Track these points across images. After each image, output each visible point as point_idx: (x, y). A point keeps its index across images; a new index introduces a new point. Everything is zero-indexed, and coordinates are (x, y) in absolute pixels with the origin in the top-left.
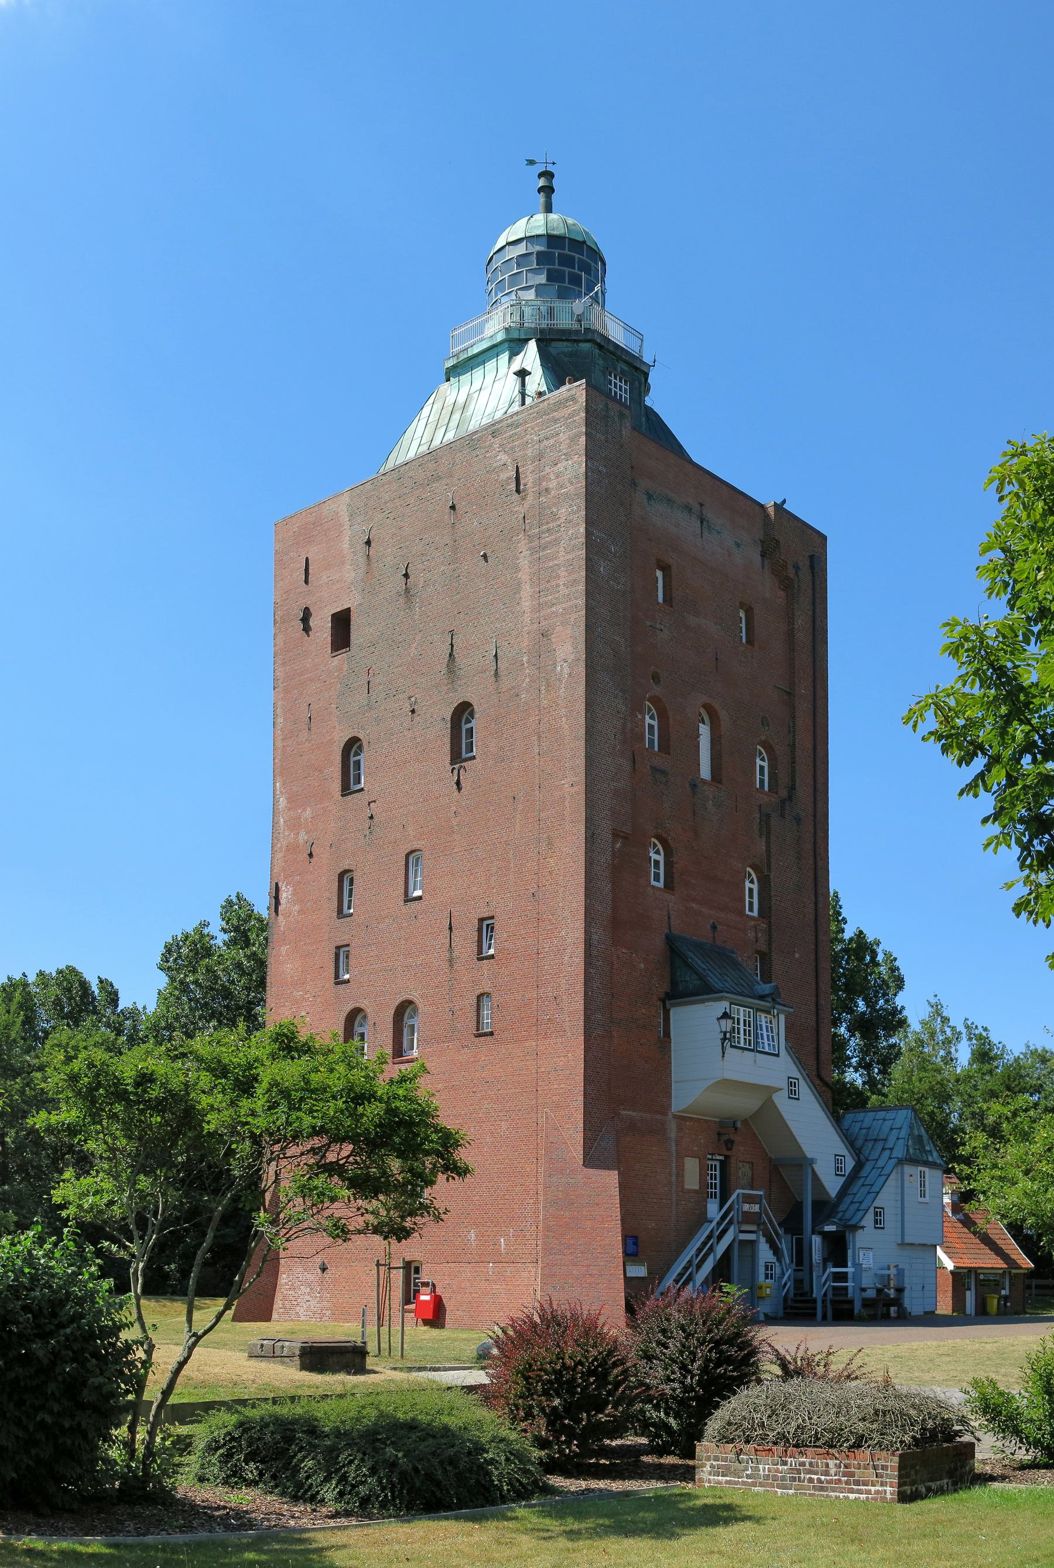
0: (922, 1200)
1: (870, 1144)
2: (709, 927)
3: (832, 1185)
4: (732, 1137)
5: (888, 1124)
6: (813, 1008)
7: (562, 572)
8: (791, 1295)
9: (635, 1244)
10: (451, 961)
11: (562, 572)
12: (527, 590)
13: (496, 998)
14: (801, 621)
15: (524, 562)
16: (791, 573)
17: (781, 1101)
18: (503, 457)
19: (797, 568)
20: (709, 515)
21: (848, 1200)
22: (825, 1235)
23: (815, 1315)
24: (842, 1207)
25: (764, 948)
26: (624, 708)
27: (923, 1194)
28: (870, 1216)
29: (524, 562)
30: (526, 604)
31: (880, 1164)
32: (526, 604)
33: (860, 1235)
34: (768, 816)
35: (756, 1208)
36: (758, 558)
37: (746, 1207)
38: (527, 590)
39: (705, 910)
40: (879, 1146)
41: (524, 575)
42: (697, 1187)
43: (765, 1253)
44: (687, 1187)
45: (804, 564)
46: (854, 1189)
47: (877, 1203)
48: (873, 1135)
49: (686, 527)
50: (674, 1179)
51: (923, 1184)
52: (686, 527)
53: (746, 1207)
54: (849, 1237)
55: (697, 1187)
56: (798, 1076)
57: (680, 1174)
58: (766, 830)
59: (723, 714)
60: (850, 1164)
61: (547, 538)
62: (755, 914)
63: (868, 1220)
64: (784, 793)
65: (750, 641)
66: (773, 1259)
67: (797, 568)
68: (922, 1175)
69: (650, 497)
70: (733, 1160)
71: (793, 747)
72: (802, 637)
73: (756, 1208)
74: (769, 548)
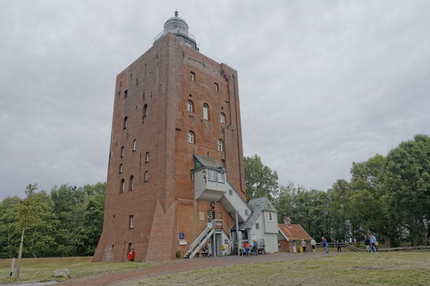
0: (271, 221)
1: (256, 207)
2: (207, 153)
3: (245, 218)
4: (214, 206)
5: (260, 201)
6: (239, 174)
7: (164, 71)
8: (233, 249)
9: (183, 235)
10: (140, 165)
11: (164, 71)
12: (158, 77)
13: (148, 172)
14: (231, 87)
15: (157, 72)
16: (228, 77)
17: (227, 195)
18: (155, 52)
19: (229, 77)
20: (206, 64)
21: (249, 221)
22: (243, 232)
23: (238, 254)
24: (247, 224)
25: (224, 159)
26: (179, 100)
27: (271, 219)
28: (255, 225)
29: (157, 72)
30: (157, 80)
31: (258, 212)
32: (157, 80)
33: (251, 231)
34: (224, 129)
35: (221, 224)
36: (219, 74)
37: (217, 224)
38: (158, 77)
39: (205, 149)
40: (258, 207)
41: (157, 74)
42: (204, 219)
43: (224, 237)
44: (200, 219)
45: (232, 76)
46: (250, 219)
47: (257, 222)
48: (257, 204)
49: (200, 67)
50: (196, 217)
51: (271, 217)
52: (200, 67)
53: (217, 224)
54: (248, 231)
55: (204, 219)
56: (232, 189)
57: (198, 216)
58: (223, 131)
59: (210, 105)
60: (250, 212)
61: (162, 65)
62: (222, 151)
63: (254, 227)
64: (228, 124)
65: (218, 90)
66: (228, 238)
67: (229, 77)
68: (270, 214)
69: (189, 59)
70: (216, 212)
71: (230, 114)
72: (232, 90)
73: (221, 224)
74: (222, 72)
